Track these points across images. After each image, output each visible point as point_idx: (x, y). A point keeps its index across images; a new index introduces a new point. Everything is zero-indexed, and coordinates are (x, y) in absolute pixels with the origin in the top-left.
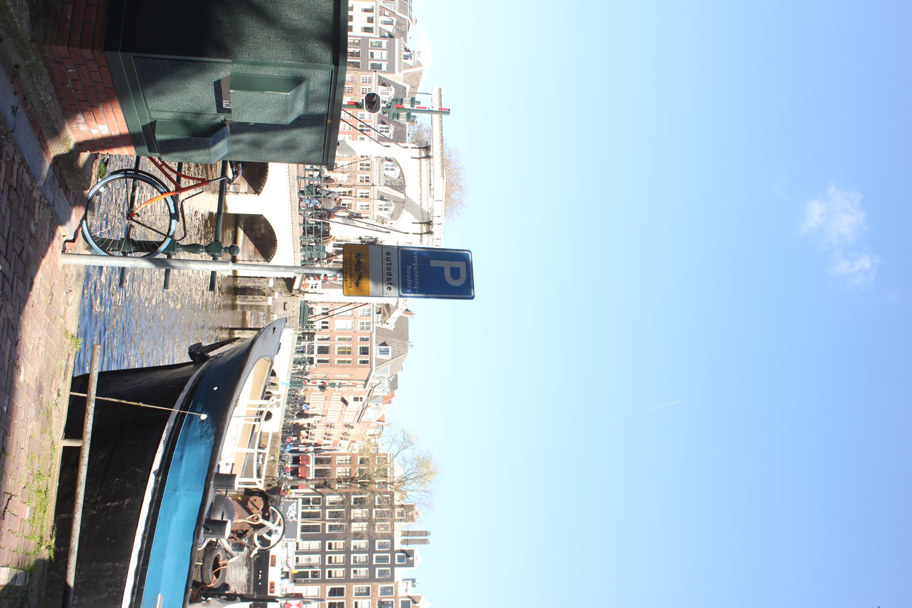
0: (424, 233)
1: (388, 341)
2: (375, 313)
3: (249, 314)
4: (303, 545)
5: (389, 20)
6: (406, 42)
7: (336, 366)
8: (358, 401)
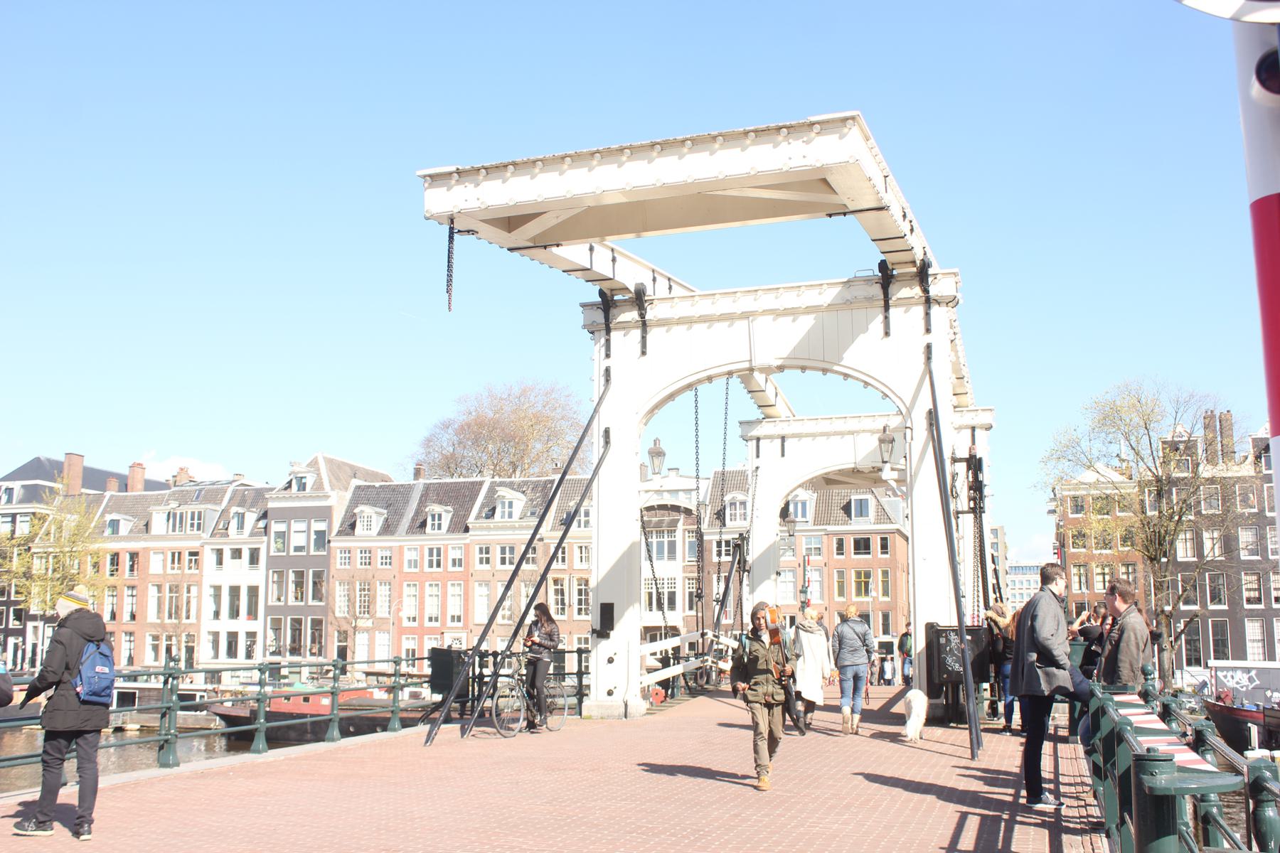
0: (926, 291)
4: (1254, 654)
5: (236, 519)
6: (274, 489)
7: (895, 599)
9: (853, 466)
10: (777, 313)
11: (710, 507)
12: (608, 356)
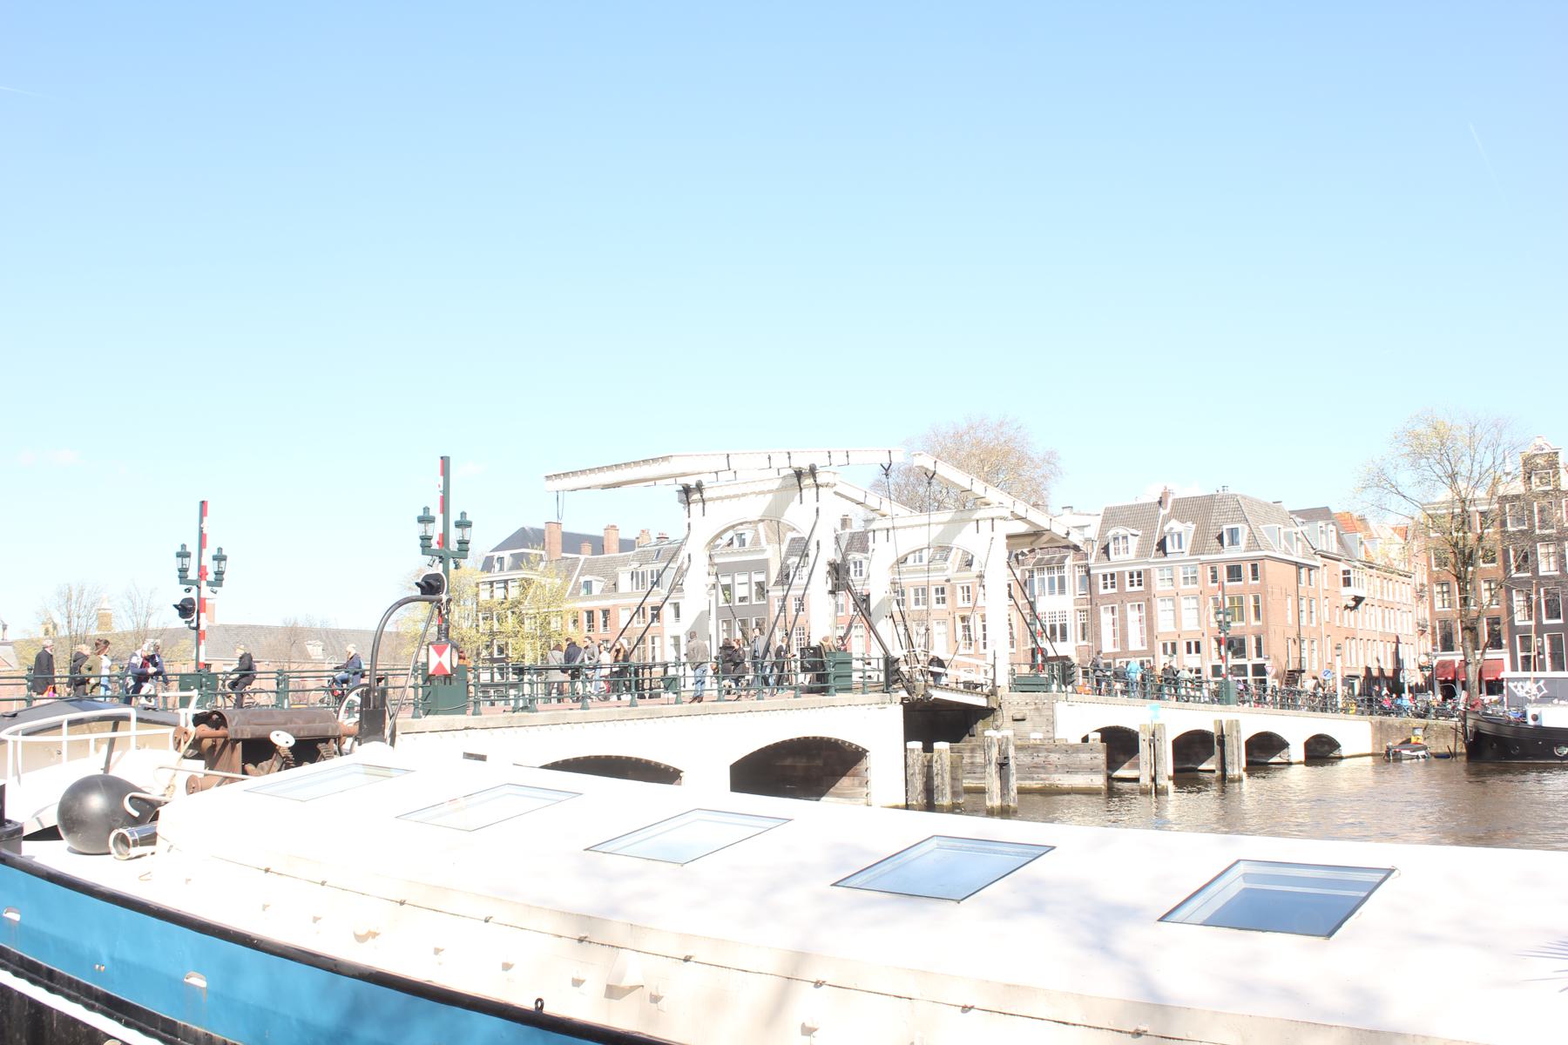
0: (815, 481)
1: (1214, 532)
2: (1165, 559)
3: (1031, 782)
7: (1266, 623)
8: (1349, 578)
11: (1098, 542)
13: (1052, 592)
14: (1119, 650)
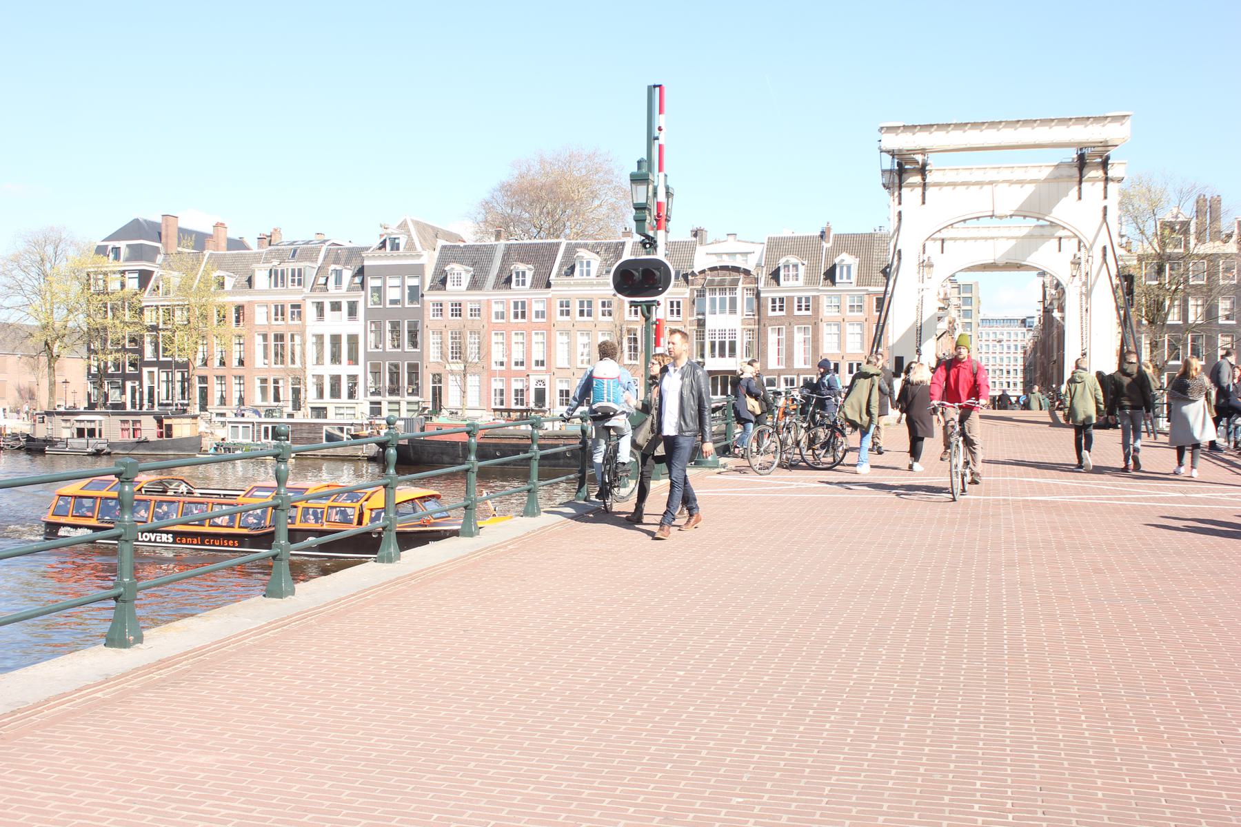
0: (1106, 173)
1: (878, 266)
2: (833, 288)
5: (334, 276)
6: (370, 248)
9: (992, 261)
10: (1011, 182)
11: (765, 269)
12: (900, 203)
13: (722, 311)
14: (783, 367)
